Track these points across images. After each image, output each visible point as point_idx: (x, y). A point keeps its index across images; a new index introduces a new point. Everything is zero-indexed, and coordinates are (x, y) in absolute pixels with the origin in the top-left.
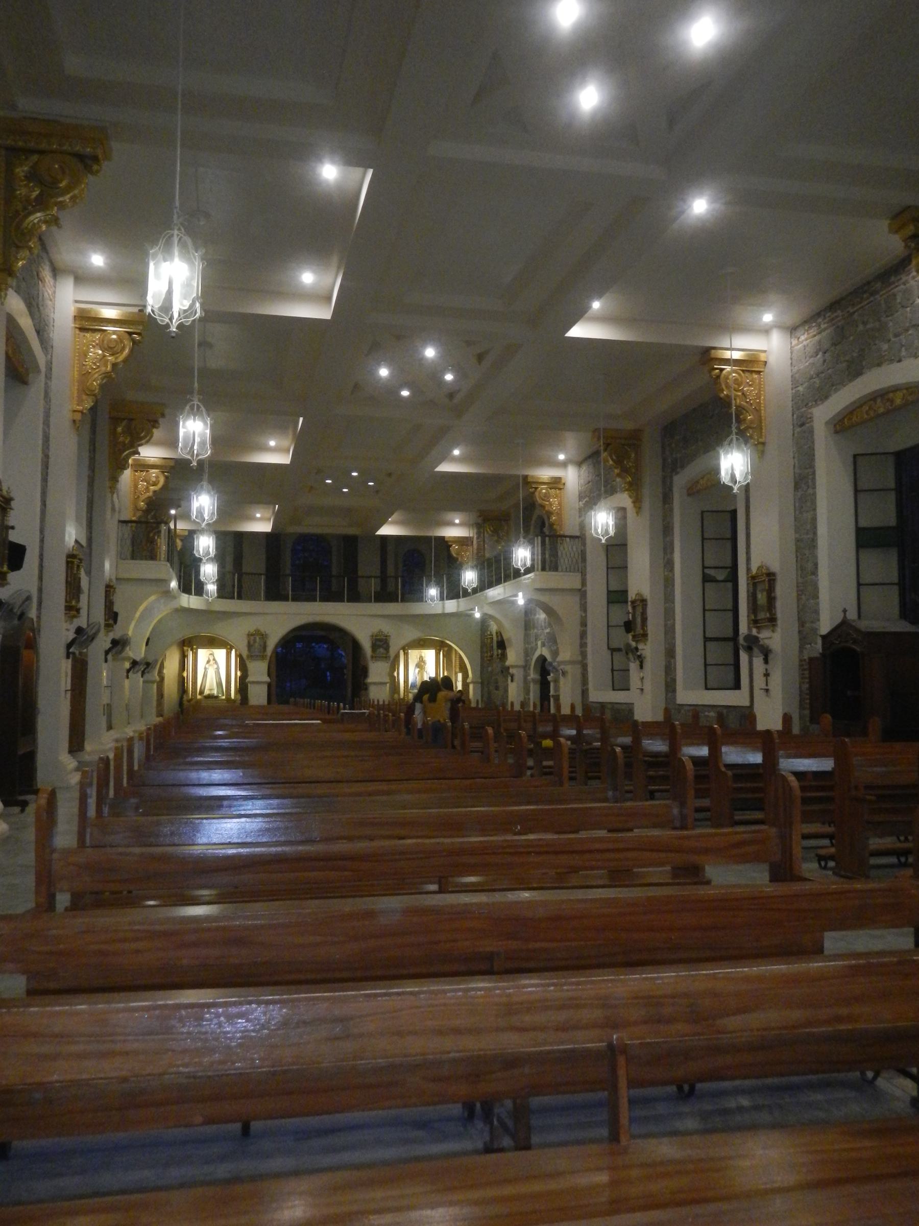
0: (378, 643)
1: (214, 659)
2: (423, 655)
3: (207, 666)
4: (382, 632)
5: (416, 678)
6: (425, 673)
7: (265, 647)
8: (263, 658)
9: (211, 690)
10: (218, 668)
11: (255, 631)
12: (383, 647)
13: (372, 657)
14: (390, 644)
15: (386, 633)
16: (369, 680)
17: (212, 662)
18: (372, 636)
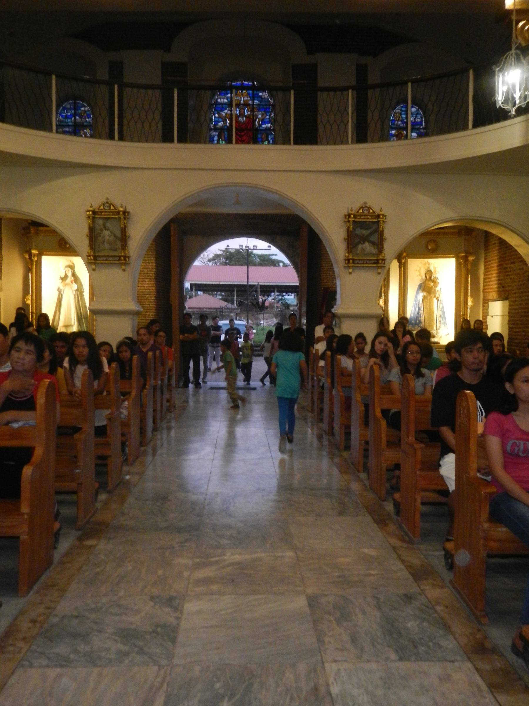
0: (359, 231)
1: (74, 275)
2: (432, 269)
4: (369, 208)
5: (419, 309)
6: (435, 300)
9: (66, 326)
11: (103, 204)
12: (370, 242)
13: (348, 260)
14: (386, 234)
15: (377, 211)
16: (337, 309)
17: (70, 278)
18: (349, 216)
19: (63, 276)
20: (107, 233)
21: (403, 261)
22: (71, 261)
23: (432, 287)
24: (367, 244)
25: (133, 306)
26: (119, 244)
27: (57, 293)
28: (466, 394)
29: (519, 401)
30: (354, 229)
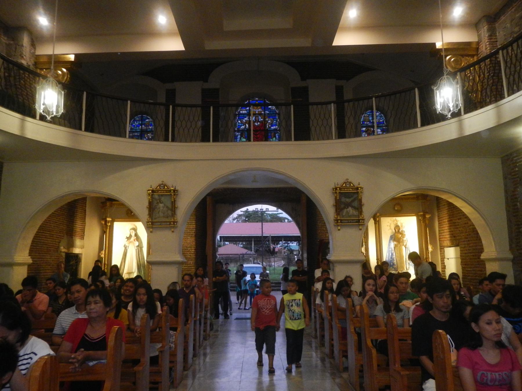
0: (343, 199)
1: (136, 235)
2: (399, 224)
3: (127, 245)
4: (350, 183)
5: (392, 254)
6: (404, 248)
7: (173, 208)
8: (172, 225)
9: (129, 273)
10: (140, 247)
11: (160, 185)
12: (352, 207)
13: (336, 220)
14: (364, 201)
15: (356, 185)
16: (332, 256)
18: (336, 189)
19: (128, 236)
20: (161, 205)
21: (378, 219)
22: (134, 225)
23: (400, 238)
24: (350, 209)
25: (179, 258)
26: (170, 212)
27: (124, 248)
28: (439, 333)
29: (484, 340)
30: (340, 199)
